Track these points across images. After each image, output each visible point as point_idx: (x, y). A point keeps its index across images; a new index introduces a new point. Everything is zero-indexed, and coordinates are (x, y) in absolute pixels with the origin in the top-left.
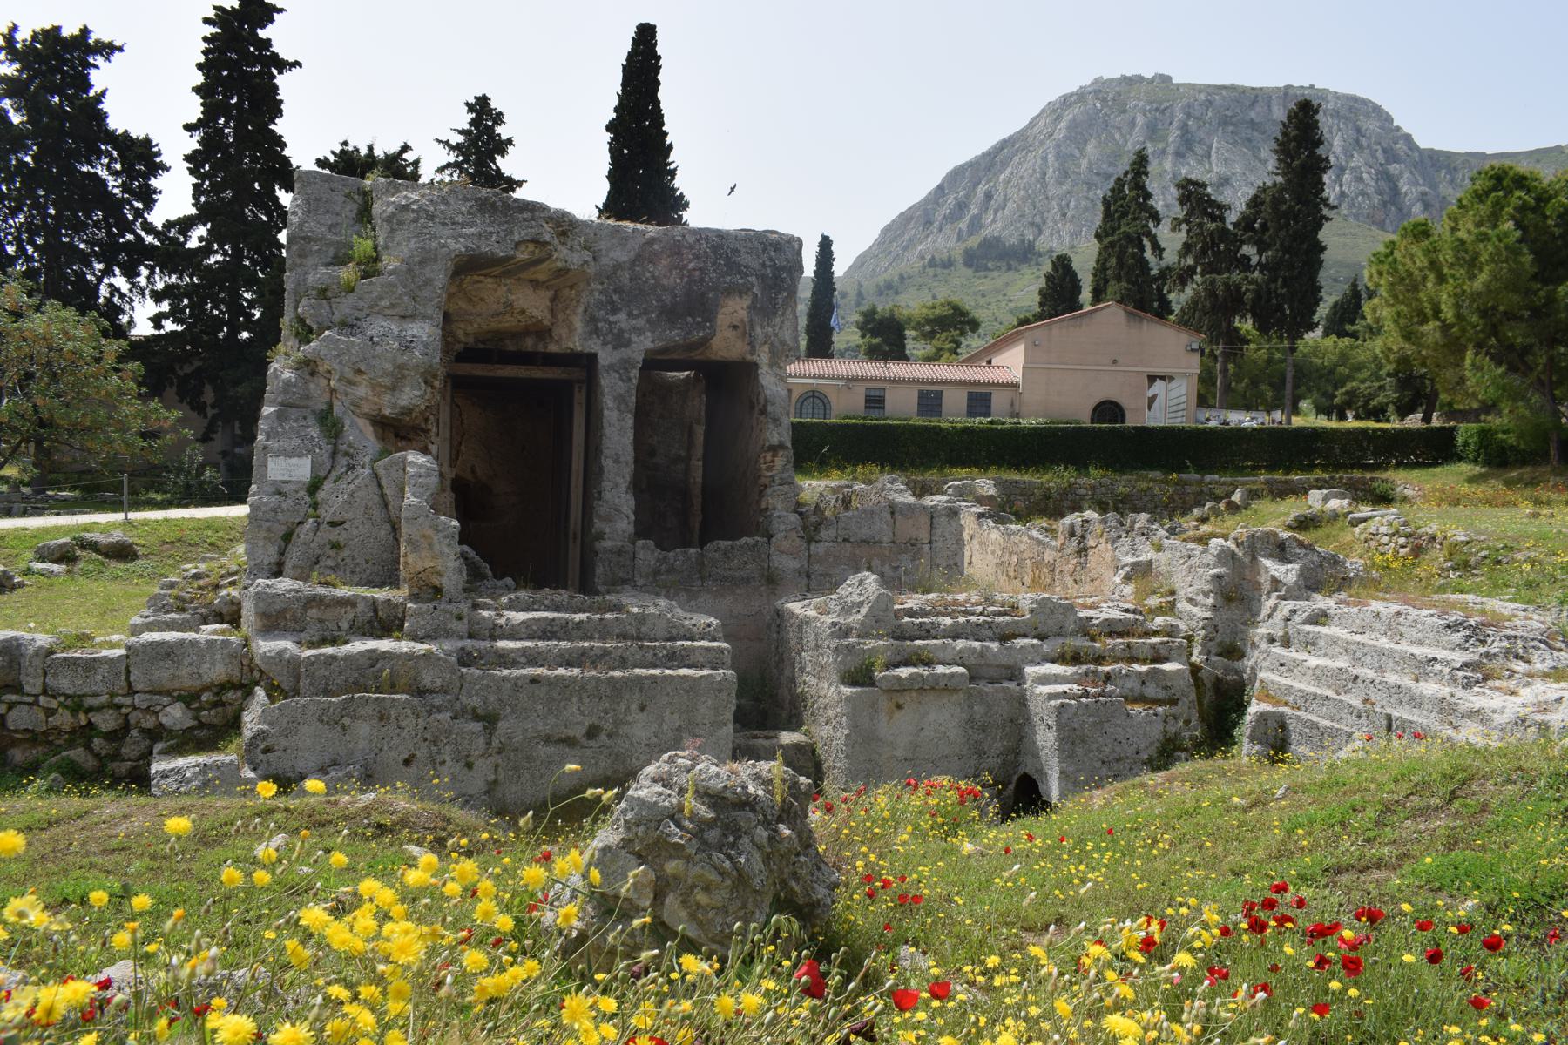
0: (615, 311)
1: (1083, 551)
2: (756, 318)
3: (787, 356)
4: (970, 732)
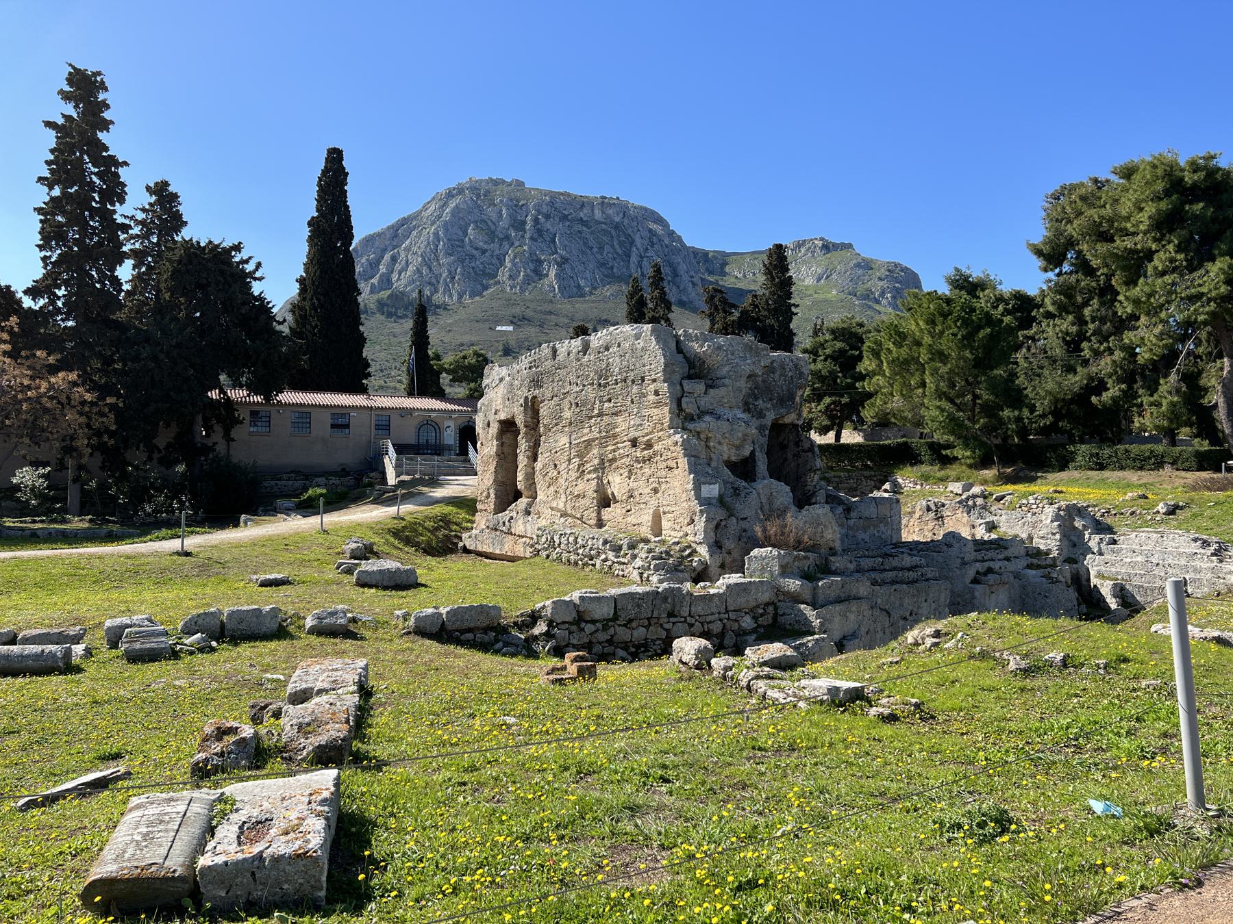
0: (756, 398)
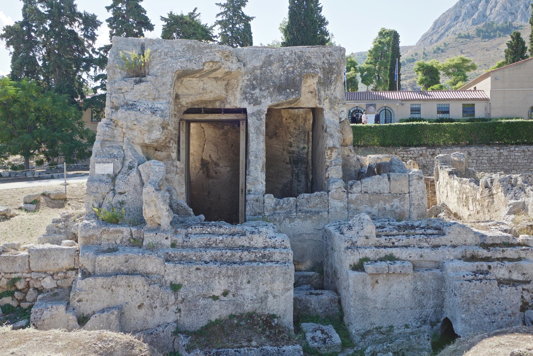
0: (254, 88)
1: (491, 195)
2: (322, 88)
3: (339, 104)
4: (416, 295)
